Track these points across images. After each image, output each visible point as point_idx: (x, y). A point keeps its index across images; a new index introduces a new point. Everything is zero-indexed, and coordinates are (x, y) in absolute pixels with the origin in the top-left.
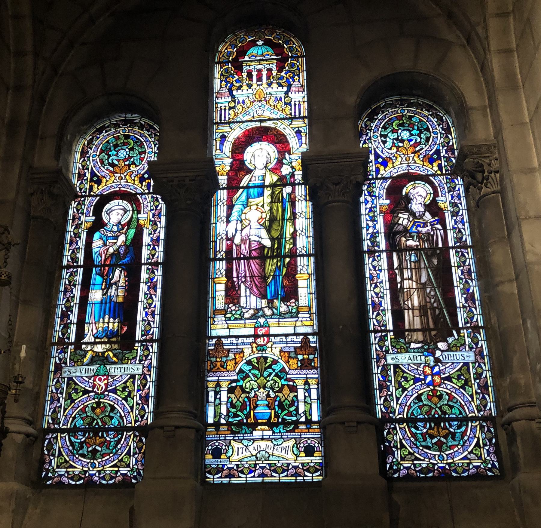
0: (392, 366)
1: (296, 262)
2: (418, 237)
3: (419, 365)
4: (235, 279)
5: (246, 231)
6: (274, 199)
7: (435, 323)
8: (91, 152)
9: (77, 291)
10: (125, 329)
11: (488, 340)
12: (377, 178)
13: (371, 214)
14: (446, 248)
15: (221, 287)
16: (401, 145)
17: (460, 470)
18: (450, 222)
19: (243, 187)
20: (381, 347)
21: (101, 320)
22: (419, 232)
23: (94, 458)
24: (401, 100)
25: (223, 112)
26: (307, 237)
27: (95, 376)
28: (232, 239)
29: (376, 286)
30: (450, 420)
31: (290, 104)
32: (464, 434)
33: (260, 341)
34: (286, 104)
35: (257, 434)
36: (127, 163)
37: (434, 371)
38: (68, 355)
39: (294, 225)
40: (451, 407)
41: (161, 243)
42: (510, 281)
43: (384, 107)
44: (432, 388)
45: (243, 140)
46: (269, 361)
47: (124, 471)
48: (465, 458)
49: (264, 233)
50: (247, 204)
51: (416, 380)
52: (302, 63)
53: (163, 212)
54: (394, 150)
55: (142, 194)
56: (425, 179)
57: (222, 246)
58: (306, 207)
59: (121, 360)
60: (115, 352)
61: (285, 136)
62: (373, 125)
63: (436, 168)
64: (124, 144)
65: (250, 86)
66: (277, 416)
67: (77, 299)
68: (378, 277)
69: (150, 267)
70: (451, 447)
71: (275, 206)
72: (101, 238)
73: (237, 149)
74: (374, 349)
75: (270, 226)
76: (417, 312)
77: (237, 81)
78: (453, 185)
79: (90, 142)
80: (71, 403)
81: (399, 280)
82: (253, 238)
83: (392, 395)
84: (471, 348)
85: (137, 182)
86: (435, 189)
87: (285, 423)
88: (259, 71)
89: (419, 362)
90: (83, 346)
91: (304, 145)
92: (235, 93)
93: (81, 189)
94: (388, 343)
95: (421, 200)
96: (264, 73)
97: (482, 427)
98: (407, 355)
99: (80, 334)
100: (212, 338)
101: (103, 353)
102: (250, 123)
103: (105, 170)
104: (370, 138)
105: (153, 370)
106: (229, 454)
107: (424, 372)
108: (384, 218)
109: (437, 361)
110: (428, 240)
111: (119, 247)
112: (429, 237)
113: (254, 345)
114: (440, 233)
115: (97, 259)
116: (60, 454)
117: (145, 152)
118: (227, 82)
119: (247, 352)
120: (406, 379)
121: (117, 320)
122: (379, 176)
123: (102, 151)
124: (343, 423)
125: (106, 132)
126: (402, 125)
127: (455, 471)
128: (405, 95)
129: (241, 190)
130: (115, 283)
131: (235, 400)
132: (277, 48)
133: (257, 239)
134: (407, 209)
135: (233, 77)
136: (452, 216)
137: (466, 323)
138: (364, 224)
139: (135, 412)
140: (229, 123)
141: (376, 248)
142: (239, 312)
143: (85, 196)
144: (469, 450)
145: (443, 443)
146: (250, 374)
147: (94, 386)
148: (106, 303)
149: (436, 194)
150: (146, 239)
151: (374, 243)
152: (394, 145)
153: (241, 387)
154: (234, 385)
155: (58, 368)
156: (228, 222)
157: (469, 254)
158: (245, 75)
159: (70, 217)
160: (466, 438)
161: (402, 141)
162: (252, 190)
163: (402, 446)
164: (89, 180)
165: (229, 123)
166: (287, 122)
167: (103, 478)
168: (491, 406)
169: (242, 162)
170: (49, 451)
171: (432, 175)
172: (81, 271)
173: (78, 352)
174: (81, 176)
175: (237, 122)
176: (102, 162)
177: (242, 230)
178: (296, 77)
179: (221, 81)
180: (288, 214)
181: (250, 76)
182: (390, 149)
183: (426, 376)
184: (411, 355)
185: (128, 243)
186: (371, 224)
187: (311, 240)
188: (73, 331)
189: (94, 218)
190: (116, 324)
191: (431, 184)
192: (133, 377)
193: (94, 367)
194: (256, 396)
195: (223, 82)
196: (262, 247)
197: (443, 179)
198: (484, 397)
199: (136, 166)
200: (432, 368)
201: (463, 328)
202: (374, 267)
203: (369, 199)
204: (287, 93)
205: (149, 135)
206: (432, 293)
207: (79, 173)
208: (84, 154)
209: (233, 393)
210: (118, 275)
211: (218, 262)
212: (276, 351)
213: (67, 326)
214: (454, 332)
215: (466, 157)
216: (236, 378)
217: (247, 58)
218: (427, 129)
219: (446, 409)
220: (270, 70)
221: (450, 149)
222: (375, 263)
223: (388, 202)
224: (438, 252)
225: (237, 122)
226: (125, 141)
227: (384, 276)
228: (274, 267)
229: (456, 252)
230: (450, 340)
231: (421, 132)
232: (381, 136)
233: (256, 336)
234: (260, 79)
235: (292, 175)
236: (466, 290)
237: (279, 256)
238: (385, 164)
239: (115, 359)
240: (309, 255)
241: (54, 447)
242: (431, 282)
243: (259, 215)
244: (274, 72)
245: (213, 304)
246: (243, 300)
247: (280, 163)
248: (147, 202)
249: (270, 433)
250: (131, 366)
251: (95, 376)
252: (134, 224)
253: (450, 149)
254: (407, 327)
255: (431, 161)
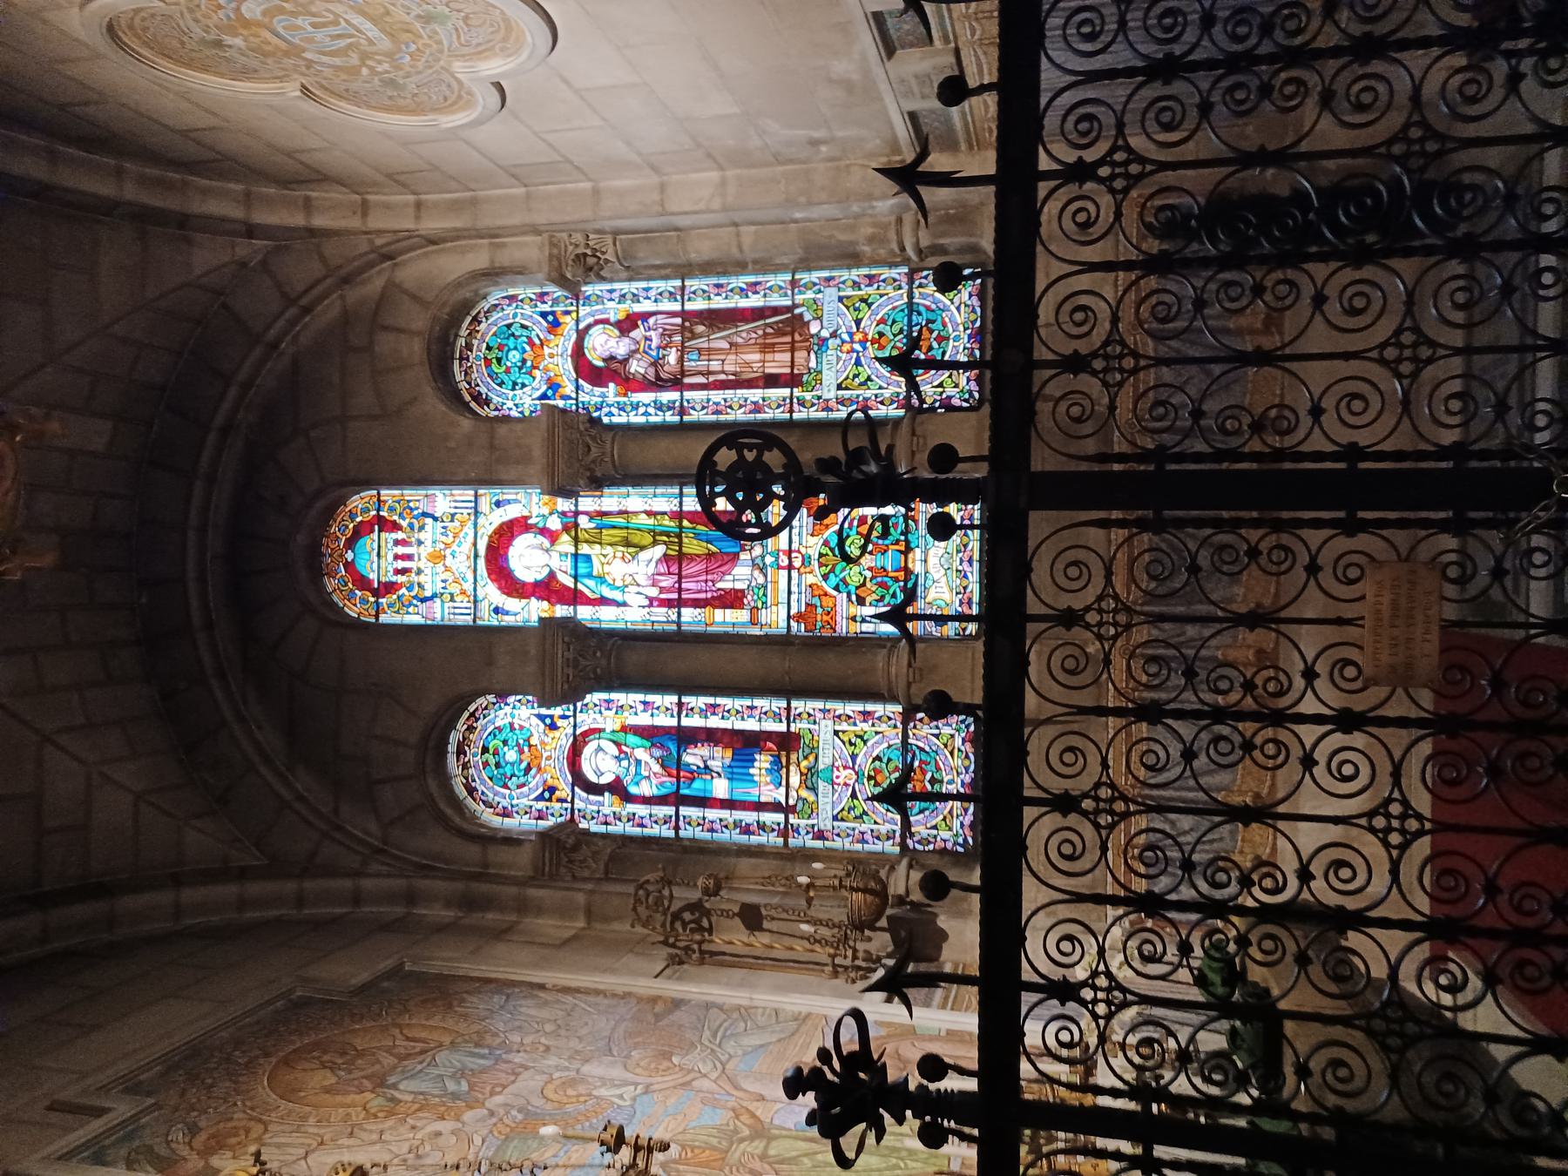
0: (840, 392)
1: (690, 512)
2: (664, 349)
3: (839, 359)
4: (709, 595)
5: (642, 580)
6: (596, 540)
7: (784, 334)
8: (505, 803)
9: (712, 814)
10: (770, 744)
11: (809, 269)
12: (577, 399)
13: (629, 408)
14: (684, 314)
15: (719, 615)
16: (529, 364)
17: (973, 317)
18: (645, 306)
19: (576, 581)
20: (813, 405)
21: (756, 778)
22: (659, 348)
23: (941, 782)
24: (461, 359)
25: (457, 611)
26: (655, 496)
27: (833, 783)
28: (651, 600)
29: (730, 407)
30: (910, 326)
31: (453, 515)
32: (928, 308)
33: (797, 563)
34: (452, 521)
35: (918, 568)
36: (526, 749)
37: (848, 339)
38: (803, 822)
39: (636, 513)
40: (894, 322)
41: (650, 698)
42: (738, 235)
43: (469, 384)
44: (869, 344)
45: (503, 583)
46: (825, 550)
47: (958, 741)
48: (958, 309)
49: (644, 555)
50: (601, 579)
51: (858, 363)
52: (386, 493)
53: (604, 696)
54: (536, 373)
55: (575, 726)
56: (582, 335)
57: (661, 614)
58: (611, 495)
59: (814, 749)
60: (801, 757)
61: (503, 524)
62: (496, 399)
63: (567, 319)
64: (496, 753)
65: (419, 572)
66: (897, 542)
67: (724, 814)
68: (717, 404)
69: (684, 713)
70: (944, 325)
71: (606, 539)
72: (637, 784)
73: (517, 591)
74: (816, 414)
75: (634, 546)
76: (769, 357)
77: (410, 589)
78: (593, 298)
79: (488, 804)
80: (867, 814)
81: (723, 377)
82: (651, 569)
83: (876, 396)
84: (820, 291)
85: (557, 734)
86: (597, 322)
87: (906, 533)
88: (397, 557)
89: (835, 358)
90: (791, 802)
91: (519, 497)
92: (428, 594)
93: (561, 815)
94: (808, 396)
95: (612, 342)
96: (401, 550)
97: (920, 286)
98: (825, 372)
99: (775, 807)
100: (789, 626)
101: (802, 774)
102: (479, 572)
103: (535, 781)
104: (516, 405)
105: (829, 705)
106: (943, 604)
107: (848, 352)
108: (635, 391)
109: (834, 335)
110: (670, 336)
111: (652, 756)
112: (666, 334)
113: (802, 570)
114: (661, 319)
115: (669, 786)
116: (935, 827)
117: (511, 725)
118: (410, 604)
119: (811, 579)
120: (856, 376)
121: (757, 757)
122: (574, 395)
123: (505, 786)
124: (913, 453)
125: (474, 781)
126: (499, 360)
127: (973, 322)
128: (453, 352)
129: (580, 587)
130: (705, 762)
131: (875, 596)
132: (360, 532)
133: (653, 564)
134: (625, 361)
135: (403, 595)
136: (639, 301)
137: (786, 295)
138: (642, 420)
139: (883, 727)
140: (475, 602)
141: (677, 404)
142: (756, 590)
143: (573, 810)
144: (948, 303)
145: (939, 335)
146: (842, 576)
147: (846, 784)
148: (732, 773)
149: (606, 321)
150: (644, 719)
151: (670, 407)
152: (530, 373)
153: (857, 588)
154: (854, 598)
155: (820, 835)
156: (625, 604)
157: (693, 284)
158: (400, 579)
159: (602, 829)
160: (934, 306)
161: (524, 361)
162: (581, 571)
163: (940, 385)
164: (548, 804)
165: (475, 602)
166: (481, 520)
167: (967, 769)
168: (894, 273)
169: (537, 584)
170: (929, 842)
171: (577, 325)
172: (684, 811)
173: (798, 809)
174: (541, 816)
175: (475, 590)
176: (520, 786)
177: (638, 585)
178: (411, 504)
179: (408, 613)
180: (620, 521)
181: (403, 571)
182: (534, 378)
183: (853, 350)
184: (825, 367)
185: (648, 744)
186: (642, 410)
187: (659, 490)
188: (769, 818)
189: (607, 794)
190: (763, 757)
191: (589, 327)
192: (836, 733)
193: (821, 785)
194: (870, 569)
195: (411, 610)
196: (666, 558)
197: (583, 311)
198: (884, 281)
199: (532, 735)
200: (843, 342)
201: (793, 300)
202: (703, 408)
203: (605, 410)
204: (435, 519)
205: (485, 717)
206: (744, 335)
207: (537, 819)
208: (506, 814)
209: (864, 599)
210: (693, 757)
211: (683, 619)
212: (812, 541)
213: (762, 827)
214: (797, 311)
215: (563, 276)
216: (845, 595)
217: (373, 576)
218: (509, 326)
219: (896, 328)
220: (397, 543)
221: (542, 297)
222: (698, 407)
223: (612, 385)
224: (687, 324)
225: (475, 590)
226: (491, 752)
227: (717, 396)
228: (695, 542)
229: (689, 300)
230: (807, 317)
231: (513, 335)
232: (513, 389)
233: (790, 567)
234: (409, 557)
235: (564, 514)
236: (743, 292)
237: (679, 536)
238: (554, 386)
239: (812, 758)
240: (681, 495)
241: (925, 836)
242: (729, 336)
243: (618, 561)
244: (400, 535)
245: (743, 625)
246: (739, 586)
247: (544, 531)
248: (586, 720)
249: (918, 551)
250: (822, 735)
251: (833, 783)
252: (621, 737)
253: (542, 297)
254: (788, 370)
255: (555, 325)
